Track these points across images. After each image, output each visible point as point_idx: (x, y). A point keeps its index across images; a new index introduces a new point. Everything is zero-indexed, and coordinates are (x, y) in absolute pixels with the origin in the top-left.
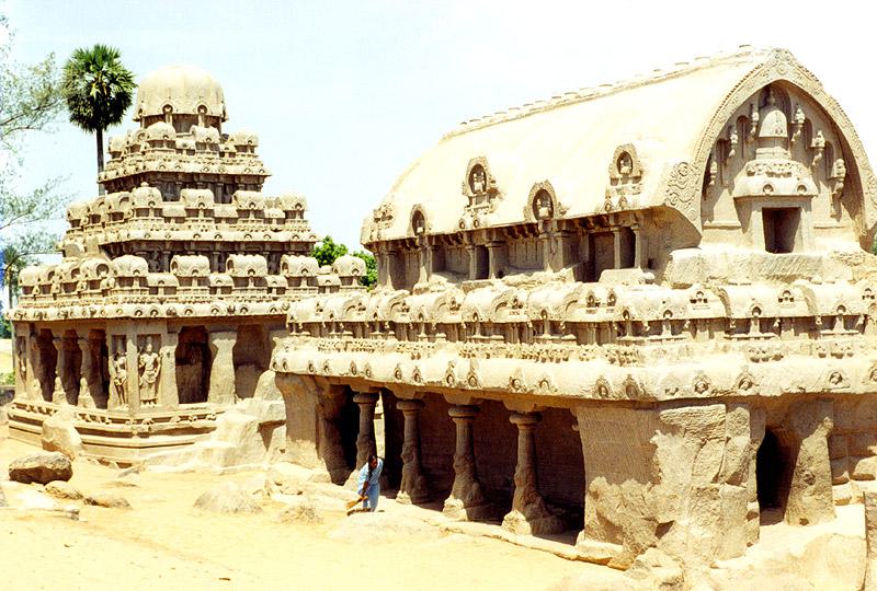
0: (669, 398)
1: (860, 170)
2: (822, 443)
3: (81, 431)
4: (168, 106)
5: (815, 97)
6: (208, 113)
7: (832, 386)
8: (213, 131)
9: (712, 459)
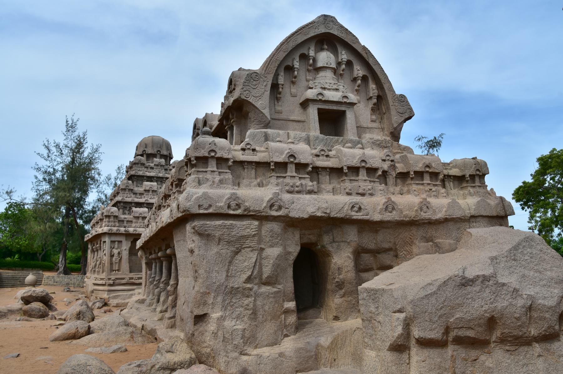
0: (201, 211)
1: (387, 91)
2: (349, 257)
3: (95, 284)
4: (144, 151)
5: (353, 45)
6: (162, 153)
7: (353, 213)
8: (163, 161)
9: (246, 264)
